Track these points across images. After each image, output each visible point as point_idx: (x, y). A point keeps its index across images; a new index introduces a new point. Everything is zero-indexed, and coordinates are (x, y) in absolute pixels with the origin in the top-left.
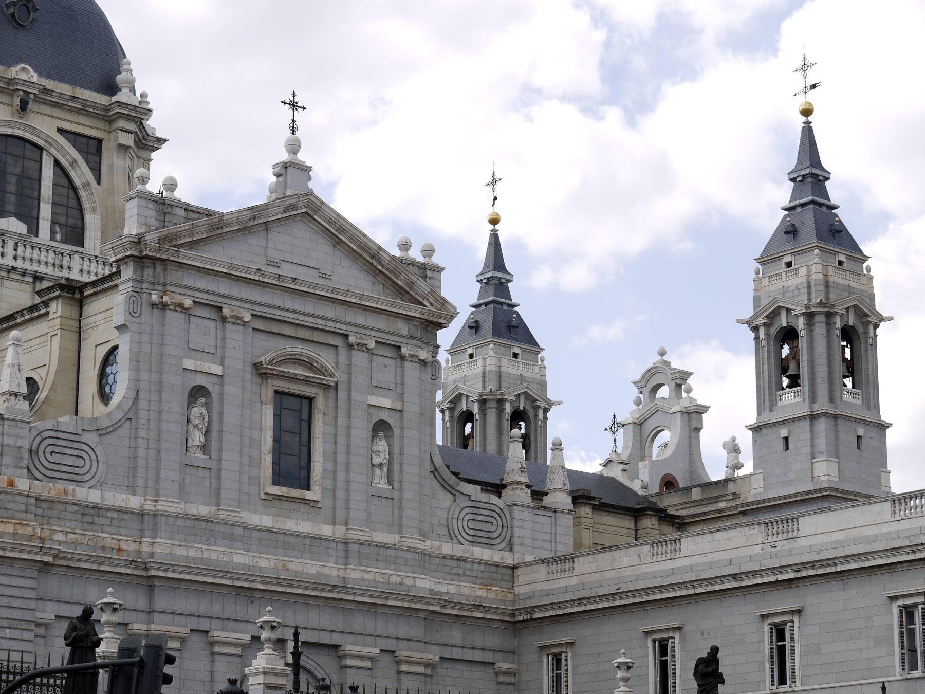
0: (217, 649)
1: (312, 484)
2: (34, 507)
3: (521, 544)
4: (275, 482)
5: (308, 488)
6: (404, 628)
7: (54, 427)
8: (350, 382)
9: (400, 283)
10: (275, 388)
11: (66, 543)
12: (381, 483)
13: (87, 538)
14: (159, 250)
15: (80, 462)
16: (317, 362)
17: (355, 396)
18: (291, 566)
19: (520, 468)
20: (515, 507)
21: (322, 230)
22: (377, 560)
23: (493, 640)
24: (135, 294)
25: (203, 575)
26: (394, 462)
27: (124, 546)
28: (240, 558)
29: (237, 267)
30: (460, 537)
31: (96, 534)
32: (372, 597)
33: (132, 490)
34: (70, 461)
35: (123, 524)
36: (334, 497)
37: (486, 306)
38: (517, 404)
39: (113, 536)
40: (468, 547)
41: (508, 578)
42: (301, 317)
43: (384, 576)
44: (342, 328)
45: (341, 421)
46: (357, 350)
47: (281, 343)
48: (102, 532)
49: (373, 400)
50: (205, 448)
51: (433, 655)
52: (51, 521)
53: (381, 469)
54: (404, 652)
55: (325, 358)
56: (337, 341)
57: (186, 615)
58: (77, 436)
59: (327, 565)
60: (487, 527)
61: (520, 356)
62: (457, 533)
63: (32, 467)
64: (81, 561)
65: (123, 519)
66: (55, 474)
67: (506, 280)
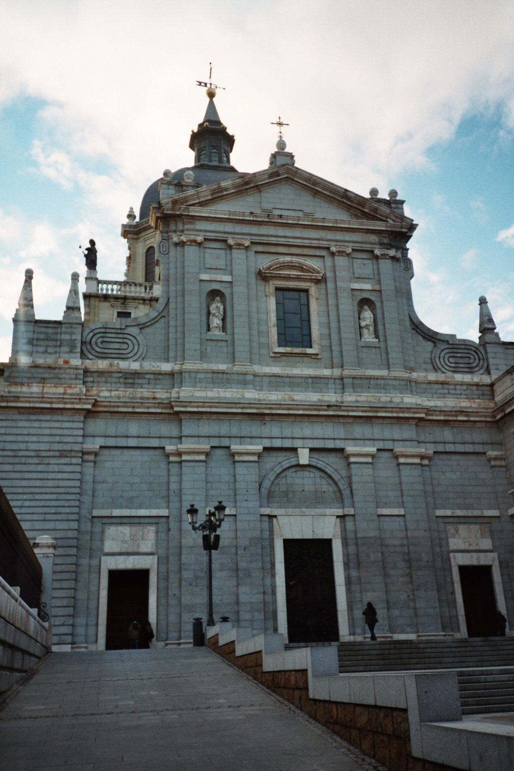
0: (237, 458)
4: (280, 345)
6: (396, 432)
9: (366, 211)
12: (369, 337)
13: (128, 393)
14: (173, 209)
15: (125, 346)
16: (306, 266)
18: (297, 397)
20: (487, 345)
22: (369, 388)
23: (481, 435)
27: (158, 396)
28: (251, 394)
29: (235, 213)
30: (443, 369)
32: (363, 411)
33: (167, 360)
34: (117, 346)
35: (158, 382)
36: (331, 351)
40: (450, 374)
41: (489, 393)
44: (324, 244)
45: (332, 301)
46: (339, 256)
47: (274, 257)
48: (142, 388)
49: (356, 286)
50: (224, 329)
51: (430, 450)
52: (100, 384)
53: (369, 329)
54: (399, 449)
57: (209, 437)
60: (466, 360)
62: (440, 366)
64: (118, 407)
65: (159, 379)
66: (104, 356)
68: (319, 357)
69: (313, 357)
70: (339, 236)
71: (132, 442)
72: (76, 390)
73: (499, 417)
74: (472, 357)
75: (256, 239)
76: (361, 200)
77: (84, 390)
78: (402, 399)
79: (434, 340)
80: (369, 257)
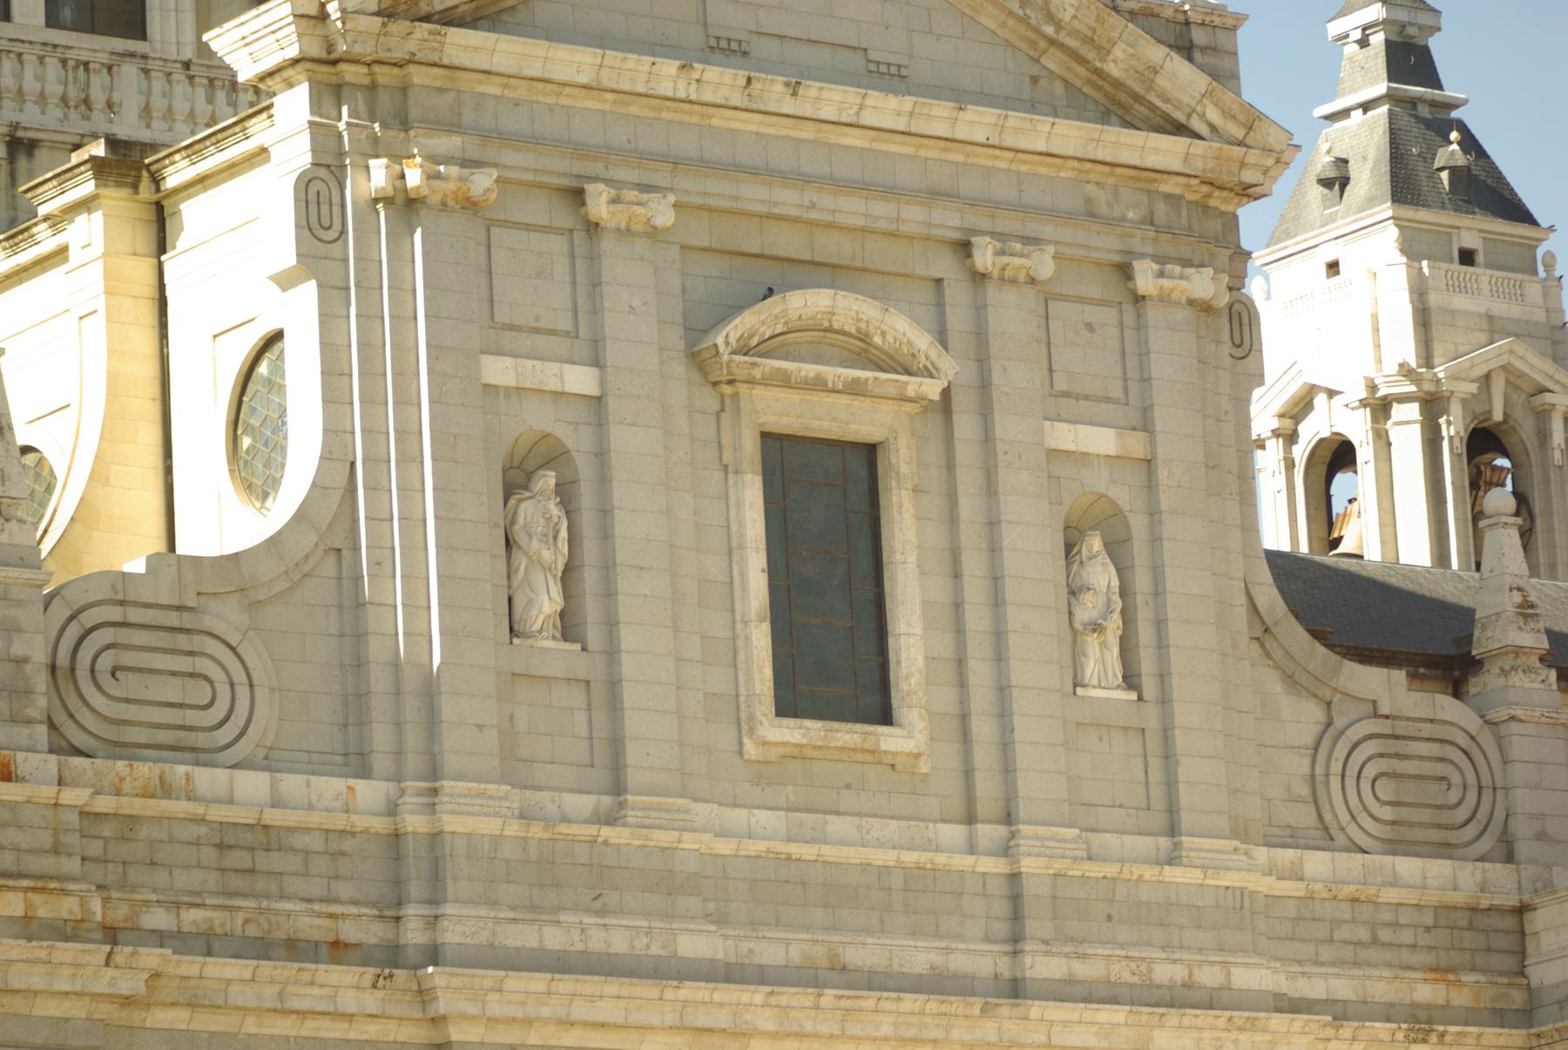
1: (895, 702)
2: (77, 836)
3: (1542, 836)
4: (786, 707)
5: (885, 717)
7: (116, 592)
8: (985, 385)
15: (201, 694)
17: (1008, 428)
19: (1520, 606)
24: (323, 172)
26: (1139, 617)
27: (349, 932)
30: (1353, 830)
31: (265, 904)
34: (170, 690)
36: (966, 737)
37: (1365, 111)
38: (1480, 408)
39: (316, 907)
41: (1506, 942)
43: (1133, 965)
45: (969, 507)
48: (283, 896)
49: (1065, 436)
56: (944, 265)
58: (186, 616)
59: (962, 946)
60: (1434, 792)
61: (1480, 258)
63: (60, 718)
65: (343, 854)
67: (1421, 27)
74: (1456, 778)
78: (1228, 975)
79: (1328, 694)
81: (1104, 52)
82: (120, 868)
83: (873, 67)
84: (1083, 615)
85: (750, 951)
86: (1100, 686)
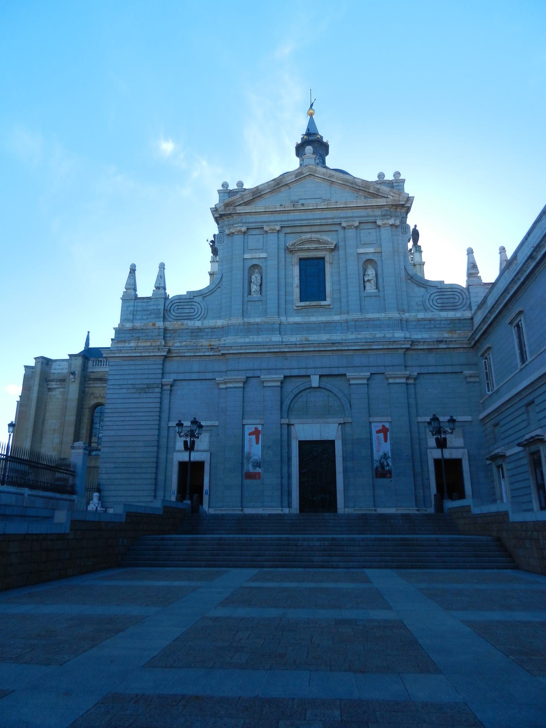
10: (299, 257)
11: (181, 346)
15: (193, 310)
16: (322, 240)
19: (473, 266)
21: (322, 180)
22: (367, 327)
24: (221, 234)
25: (249, 349)
30: (431, 309)
32: (360, 346)
33: (220, 318)
34: (187, 311)
40: (438, 313)
42: (312, 221)
43: (371, 335)
44: (337, 221)
48: (202, 339)
55: (325, 237)
56: (337, 228)
57: (246, 370)
60: (451, 300)
64: (184, 352)
65: (214, 332)
68: (331, 307)
69: (326, 307)
70: (349, 213)
71: (195, 376)
72: (158, 343)
73: (472, 344)
74: (457, 297)
75: (285, 224)
76: (367, 184)
77: (163, 343)
78: (394, 335)
79: (426, 286)
80: (374, 227)
81: (369, 189)
82: (173, 338)
83: (323, 200)
84: (366, 279)
85: (289, 339)
86: (370, 290)
